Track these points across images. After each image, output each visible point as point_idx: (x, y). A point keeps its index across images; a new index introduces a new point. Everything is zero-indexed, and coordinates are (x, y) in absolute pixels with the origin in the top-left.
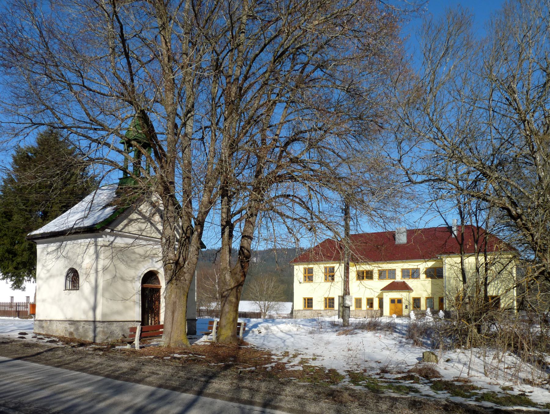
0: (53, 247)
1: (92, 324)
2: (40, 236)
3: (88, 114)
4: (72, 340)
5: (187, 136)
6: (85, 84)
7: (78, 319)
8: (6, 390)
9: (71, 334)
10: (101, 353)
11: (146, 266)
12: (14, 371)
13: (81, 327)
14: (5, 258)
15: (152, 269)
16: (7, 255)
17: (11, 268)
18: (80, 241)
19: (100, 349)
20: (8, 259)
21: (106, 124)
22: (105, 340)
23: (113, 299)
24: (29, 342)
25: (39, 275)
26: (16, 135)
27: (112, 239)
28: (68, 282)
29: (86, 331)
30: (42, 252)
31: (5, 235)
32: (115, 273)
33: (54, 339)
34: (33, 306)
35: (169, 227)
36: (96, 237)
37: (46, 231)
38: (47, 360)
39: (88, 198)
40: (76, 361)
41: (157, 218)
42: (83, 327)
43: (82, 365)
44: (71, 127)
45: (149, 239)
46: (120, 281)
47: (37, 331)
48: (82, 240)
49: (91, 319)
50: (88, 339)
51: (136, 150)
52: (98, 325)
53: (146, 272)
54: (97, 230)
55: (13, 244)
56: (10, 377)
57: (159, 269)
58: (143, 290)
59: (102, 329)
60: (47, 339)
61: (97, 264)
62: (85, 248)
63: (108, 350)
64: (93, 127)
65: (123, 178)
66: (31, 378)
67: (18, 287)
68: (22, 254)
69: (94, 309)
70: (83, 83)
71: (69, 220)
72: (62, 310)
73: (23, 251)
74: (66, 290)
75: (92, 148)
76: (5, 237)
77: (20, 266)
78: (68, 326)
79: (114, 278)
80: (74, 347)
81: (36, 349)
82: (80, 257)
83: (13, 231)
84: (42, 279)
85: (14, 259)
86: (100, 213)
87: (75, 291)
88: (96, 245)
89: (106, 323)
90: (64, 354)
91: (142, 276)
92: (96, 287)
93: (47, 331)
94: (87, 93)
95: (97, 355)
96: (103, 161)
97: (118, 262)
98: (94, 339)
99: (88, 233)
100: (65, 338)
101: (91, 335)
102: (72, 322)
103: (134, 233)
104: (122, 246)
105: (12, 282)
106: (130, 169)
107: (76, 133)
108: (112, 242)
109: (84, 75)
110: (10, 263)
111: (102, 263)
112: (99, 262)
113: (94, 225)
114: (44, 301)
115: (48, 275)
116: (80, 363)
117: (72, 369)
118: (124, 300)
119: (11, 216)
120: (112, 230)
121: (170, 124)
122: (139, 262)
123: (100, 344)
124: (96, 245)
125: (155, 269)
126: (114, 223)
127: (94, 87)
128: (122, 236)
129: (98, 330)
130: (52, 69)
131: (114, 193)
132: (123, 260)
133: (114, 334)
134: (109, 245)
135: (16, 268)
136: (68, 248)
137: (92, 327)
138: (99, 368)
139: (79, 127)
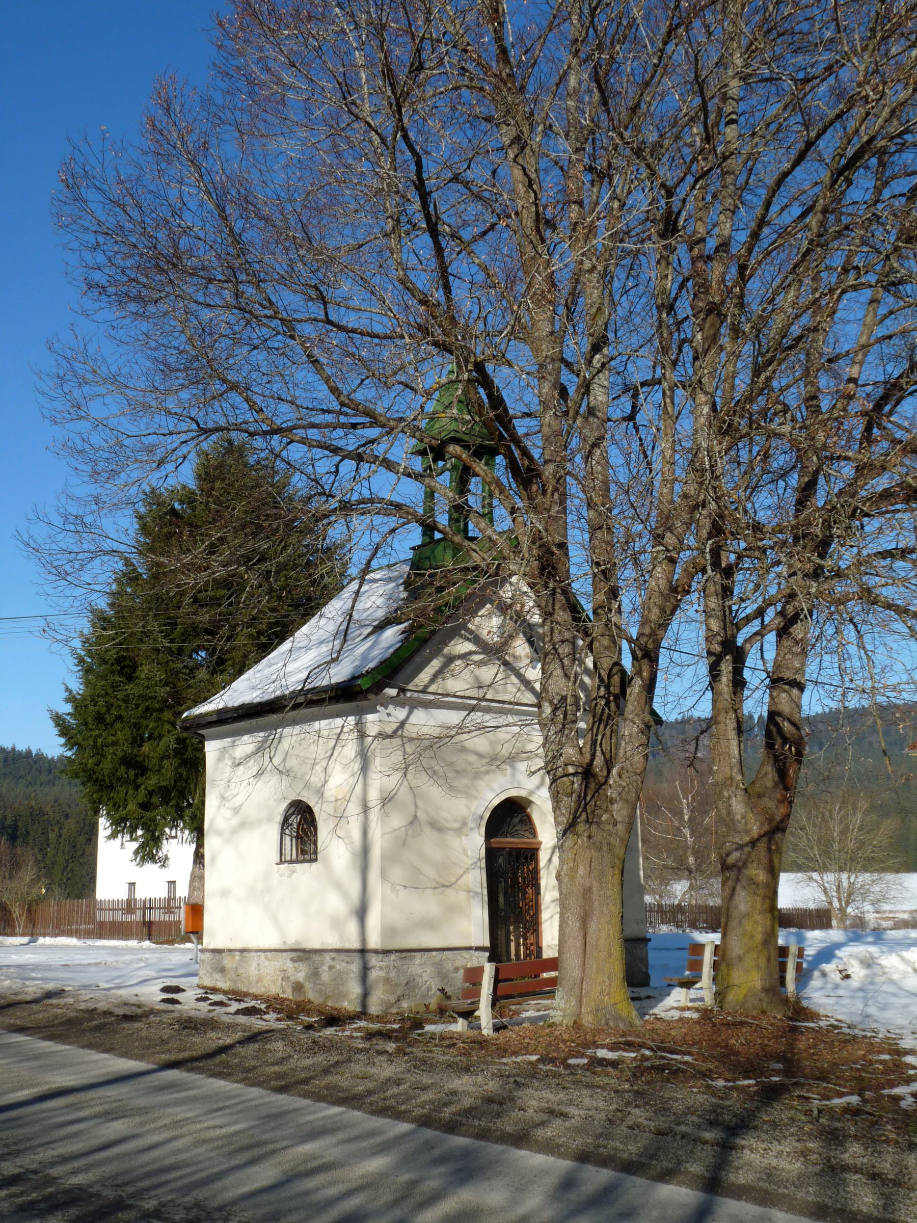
0: (246, 744)
1: (357, 958)
2: (214, 718)
3: (335, 391)
4: (302, 1007)
5: (595, 416)
6: (333, 317)
7: (317, 946)
8: (157, 1166)
9: (298, 987)
10: (391, 1046)
11: (496, 786)
12: (167, 1105)
13: (325, 968)
14: (119, 779)
15: (513, 793)
16: (123, 769)
17: (131, 806)
18: (316, 725)
19: (386, 1036)
20: (126, 782)
21: (380, 410)
22: (392, 1006)
23: (414, 884)
24: (193, 1013)
25: (211, 824)
26: (161, 463)
27: (400, 713)
28: (287, 839)
29: (339, 979)
30: (220, 760)
31: (120, 718)
32: (413, 809)
33: (253, 1003)
34: (196, 910)
35: (559, 672)
36: (360, 713)
37: (230, 705)
38: (248, 1071)
39: (335, 608)
40: (326, 1071)
41: (521, 648)
42: (331, 967)
43: (345, 1084)
44: (290, 429)
45: (504, 708)
46: (427, 830)
47: (207, 982)
48: (324, 723)
49: (355, 944)
50: (346, 1004)
51: (454, 467)
52: (374, 960)
53: (496, 802)
54: (361, 692)
55: (138, 741)
56: (160, 1123)
57: (532, 792)
58: (491, 854)
59: (382, 974)
60: (235, 1006)
61: (365, 785)
62: (332, 743)
63: (405, 1038)
64: (343, 419)
65: (423, 545)
66: (215, 1127)
67: (152, 858)
68: (161, 767)
69: (361, 913)
70: (326, 314)
71: (289, 668)
72: (274, 919)
73: (162, 759)
74: (281, 862)
75: (341, 474)
76: (118, 725)
77: (156, 800)
78: (289, 965)
79: (412, 823)
80: (309, 1027)
81: (213, 1035)
82: (318, 768)
83: (137, 706)
84: (219, 833)
85: (139, 780)
86: (368, 644)
87: (306, 865)
88: (362, 735)
89: (393, 957)
90: (289, 1050)
91: (487, 815)
92: (365, 851)
93: (235, 982)
94: (336, 338)
95: (381, 1053)
96: (367, 507)
97: (424, 778)
98: (364, 1005)
99: (337, 702)
100: (283, 1000)
101: (355, 989)
102: (302, 954)
103: (467, 693)
104: (436, 732)
105: (135, 845)
106: (442, 520)
107: (303, 441)
108: (402, 724)
109: (329, 294)
110: (131, 792)
111: (378, 784)
112: (370, 782)
113: (354, 678)
114: (225, 894)
115: (235, 822)
116: (343, 1080)
117: (318, 1097)
118: (442, 886)
119: (134, 667)
120: (403, 690)
121: (546, 388)
122: (477, 775)
123: (379, 1019)
124: (362, 735)
125: (523, 793)
126: (408, 670)
127: (351, 320)
128: (428, 705)
129: (374, 975)
130: (250, 290)
131: (402, 588)
132: (435, 772)
133: (414, 987)
134: (395, 732)
135: (145, 806)
136: (285, 744)
137: (355, 967)
138: (394, 1096)
139: (313, 426)
